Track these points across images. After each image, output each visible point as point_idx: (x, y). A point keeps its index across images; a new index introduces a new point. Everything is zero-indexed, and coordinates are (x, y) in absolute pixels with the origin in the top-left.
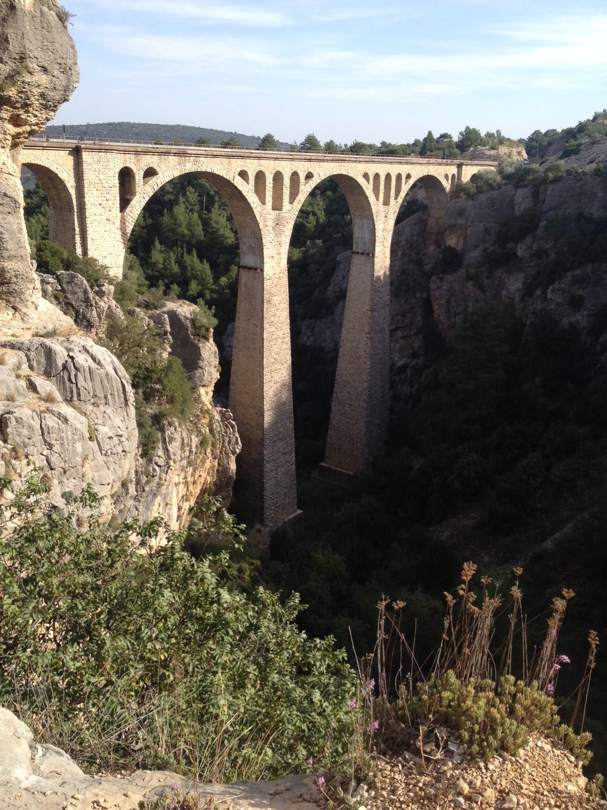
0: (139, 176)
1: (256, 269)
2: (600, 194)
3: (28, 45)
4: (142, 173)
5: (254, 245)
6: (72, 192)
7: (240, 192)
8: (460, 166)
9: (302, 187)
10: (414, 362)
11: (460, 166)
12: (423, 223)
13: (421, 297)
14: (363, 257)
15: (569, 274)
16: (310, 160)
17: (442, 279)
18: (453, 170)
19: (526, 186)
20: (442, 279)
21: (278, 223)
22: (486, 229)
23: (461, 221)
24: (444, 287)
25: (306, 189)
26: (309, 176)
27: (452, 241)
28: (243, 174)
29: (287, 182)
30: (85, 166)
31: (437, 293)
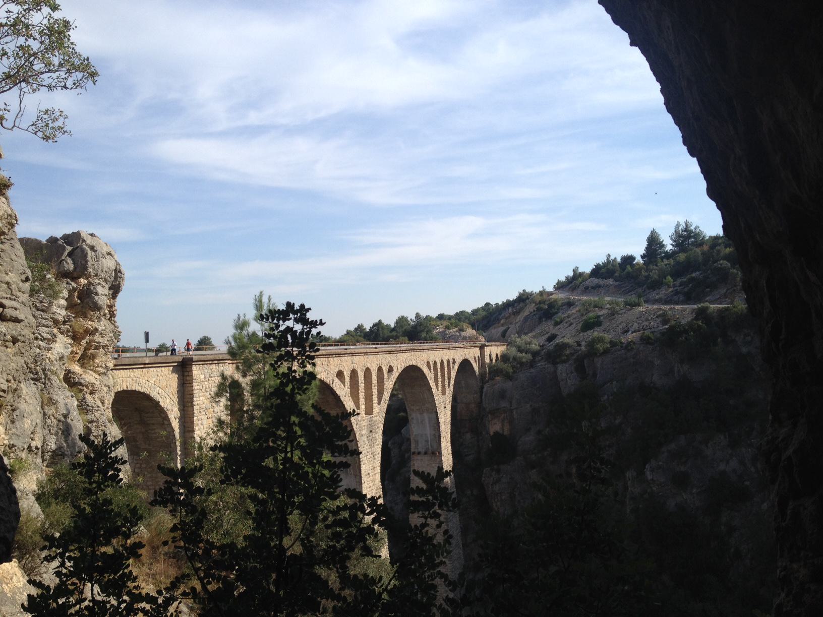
2: (657, 362)
6: (175, 424)
8: (482, 348)
9: (386, 383)
11: (482, 348)
14: (426, 458)
16: (390, 352)
17: (498, 471)
18: (476, 352)
19: (564, 362)
20: (498, 471)
23: (504, 404)
26: (390, 370)
30: (196, 386)
31: (497, 488)
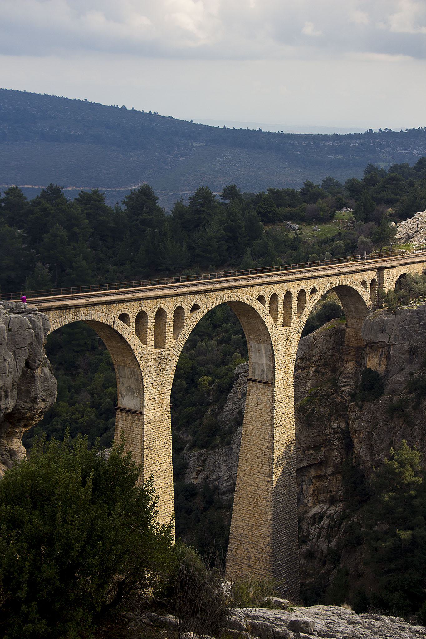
1: (135, 412)
3: (39, 392)
5: (133, 386)
7: (121, 336)
8: (381, 270)
9: (186, 322)
10: (332, 510)
12: (339, 334)
13: (339, 427)
14: (261, 386)
17: (361, 408)
20: (361, 408)
21: (161, 361)
22: (411, 348)
23: (383, 338)
24: (363, 418)
25: (191, 321)
26: (195, 308)
27: (373, 362)
28: (124, 317)
29: (170, 318)
31: (356, 425)
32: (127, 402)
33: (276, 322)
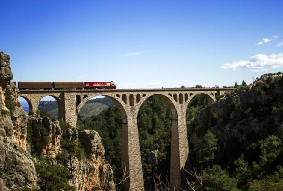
0: (82, 97)
4: (83, 96)
14: (175, 121)
15: (239, 122)
26: (144, 95)
32: (124, 121)
33: (177, 102)
